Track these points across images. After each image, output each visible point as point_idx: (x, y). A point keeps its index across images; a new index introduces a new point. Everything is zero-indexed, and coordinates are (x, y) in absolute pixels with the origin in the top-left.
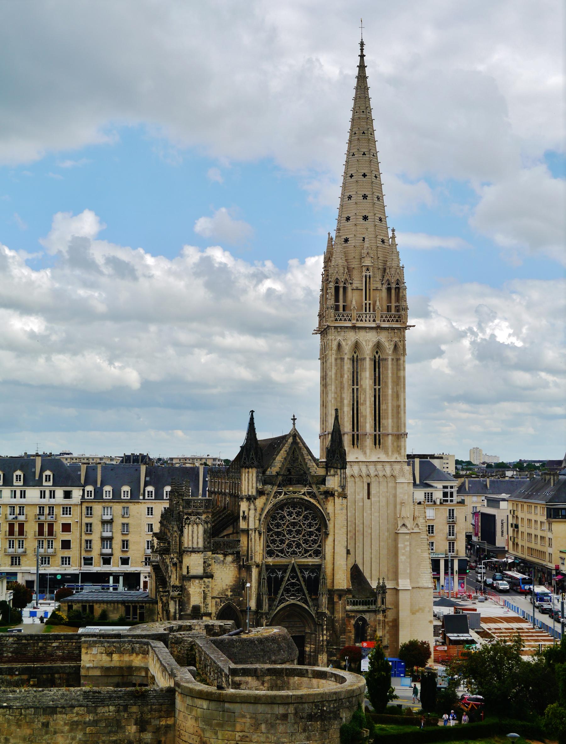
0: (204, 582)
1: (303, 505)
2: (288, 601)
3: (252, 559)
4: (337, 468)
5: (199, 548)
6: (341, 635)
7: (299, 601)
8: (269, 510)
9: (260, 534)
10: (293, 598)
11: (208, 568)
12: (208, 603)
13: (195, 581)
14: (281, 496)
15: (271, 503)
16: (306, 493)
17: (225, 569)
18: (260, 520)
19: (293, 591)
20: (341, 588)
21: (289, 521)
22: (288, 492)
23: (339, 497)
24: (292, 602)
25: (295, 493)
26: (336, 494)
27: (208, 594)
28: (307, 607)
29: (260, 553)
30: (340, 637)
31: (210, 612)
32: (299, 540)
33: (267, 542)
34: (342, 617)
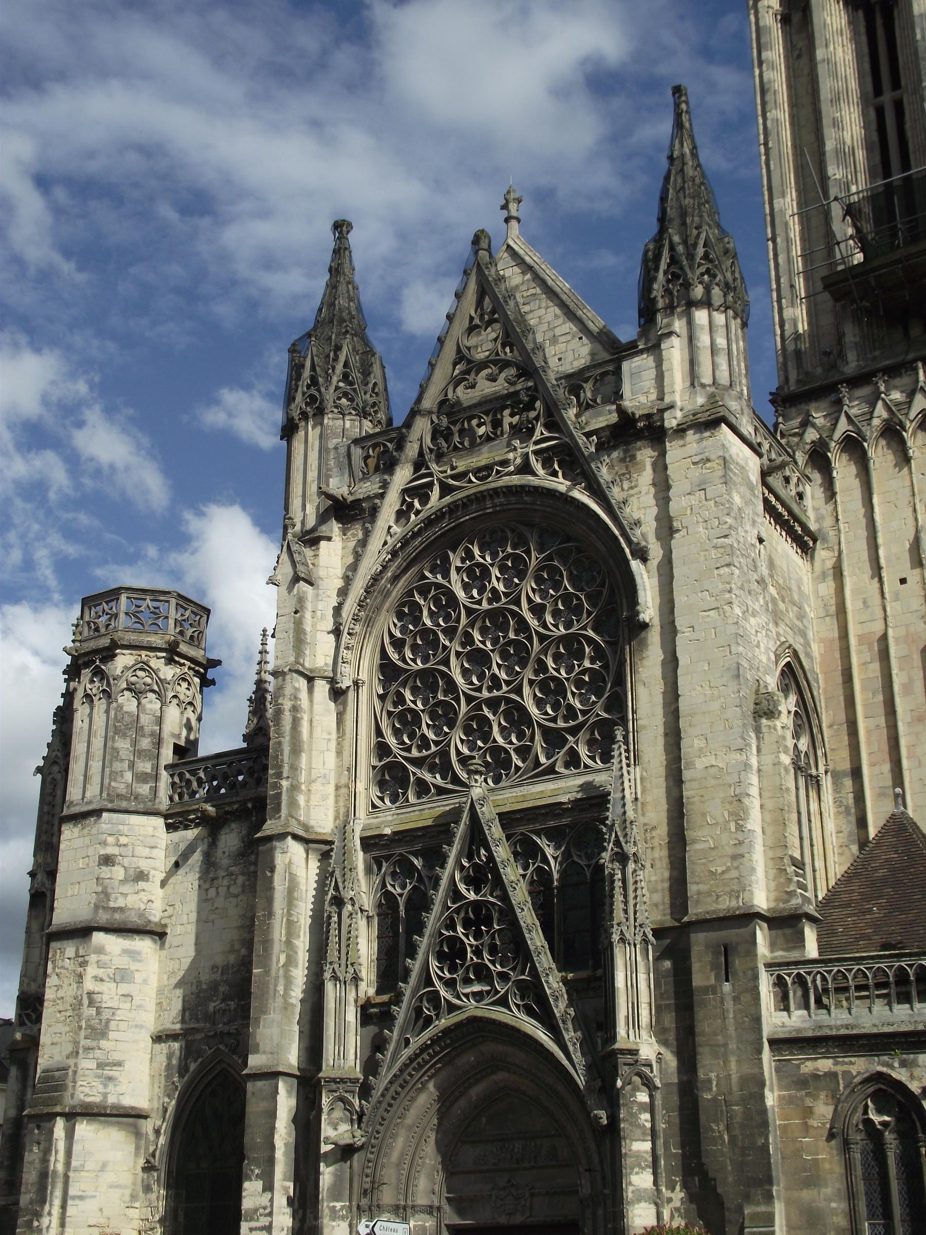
0: (100, 950)
1: (530, 525)
2: (452, 1008)
3: (278, 809)
4: (670, 309)
5: (90, 802)
6: (747, 1198)
7: (503, 1002)
8: (376, 579)
9: (337, 694)
10: (476, 988)
11: (126, 889)
12: (116, 1056)
13: (63, 953)
14: (429, 506)
15: (385, 543)
16: (532, 458)
17: (212, 892)
18: (337, 632)
19: (478, 952)
20: (725, 905)
21: (469, 611)
22: (453, 477)
23: (681, 431)
24: (472, 1008)
25: (484, 472)
26: (671, 421)
27: (120, 1015)
28: (542, 1036)
29: (337, 788)
30: (740, 1210)
31: (128, 1101)
32: (519, 691)
33: (379, 733)
34: (744, 1081)
